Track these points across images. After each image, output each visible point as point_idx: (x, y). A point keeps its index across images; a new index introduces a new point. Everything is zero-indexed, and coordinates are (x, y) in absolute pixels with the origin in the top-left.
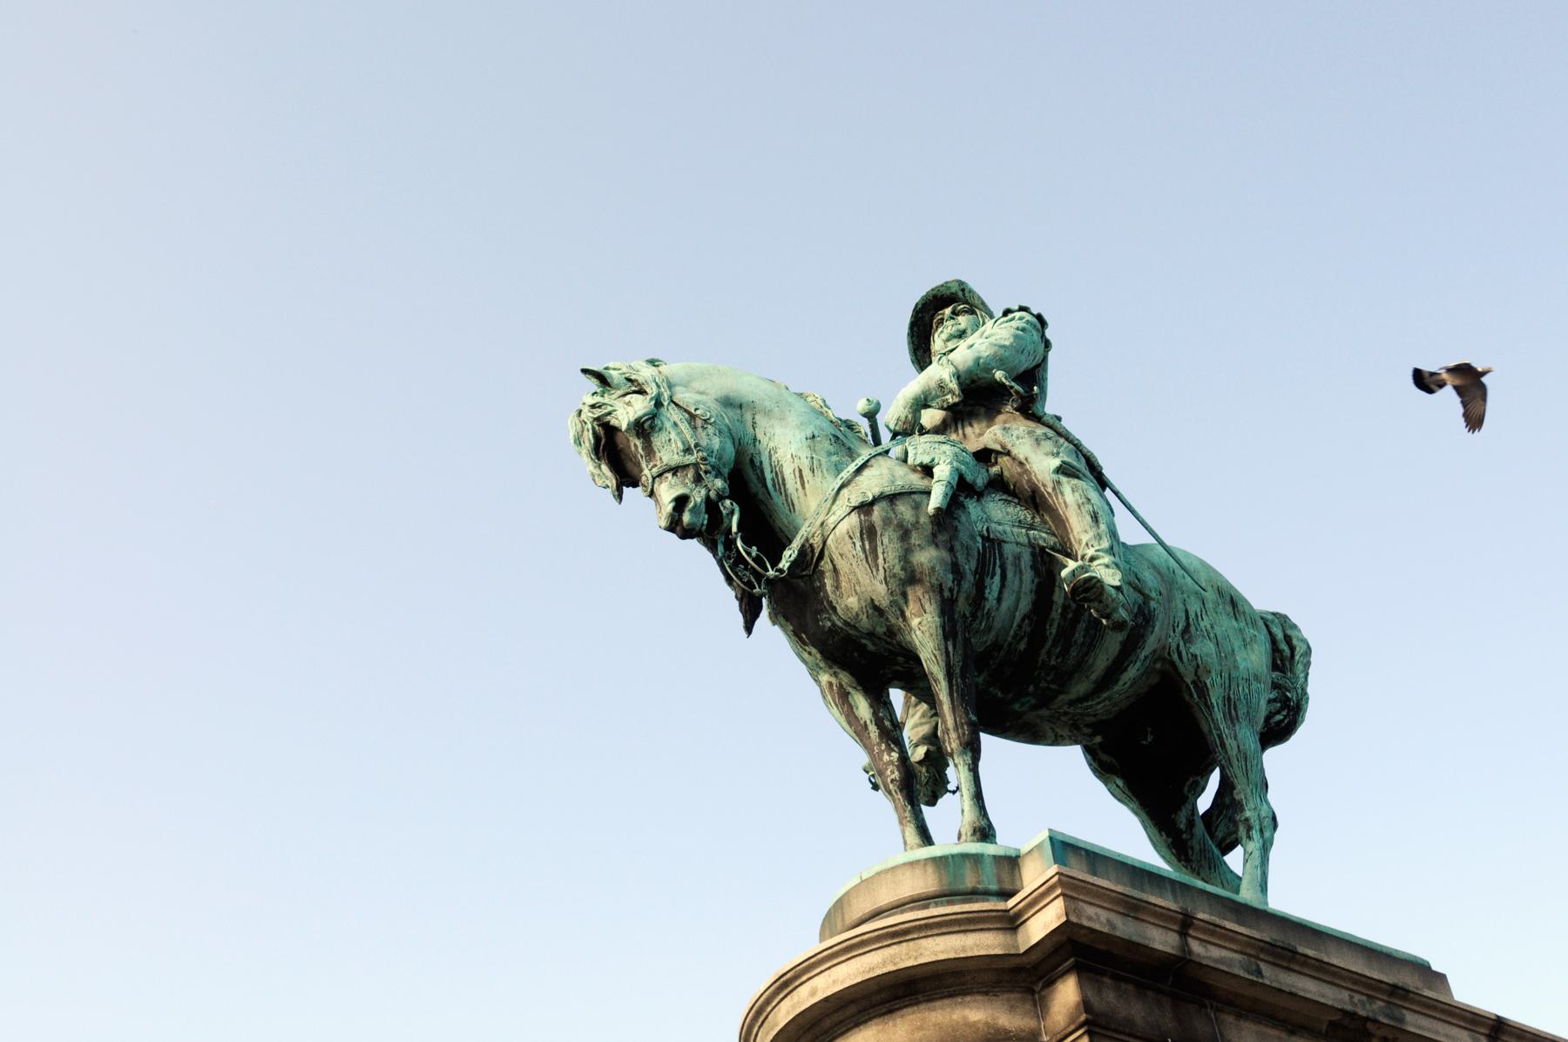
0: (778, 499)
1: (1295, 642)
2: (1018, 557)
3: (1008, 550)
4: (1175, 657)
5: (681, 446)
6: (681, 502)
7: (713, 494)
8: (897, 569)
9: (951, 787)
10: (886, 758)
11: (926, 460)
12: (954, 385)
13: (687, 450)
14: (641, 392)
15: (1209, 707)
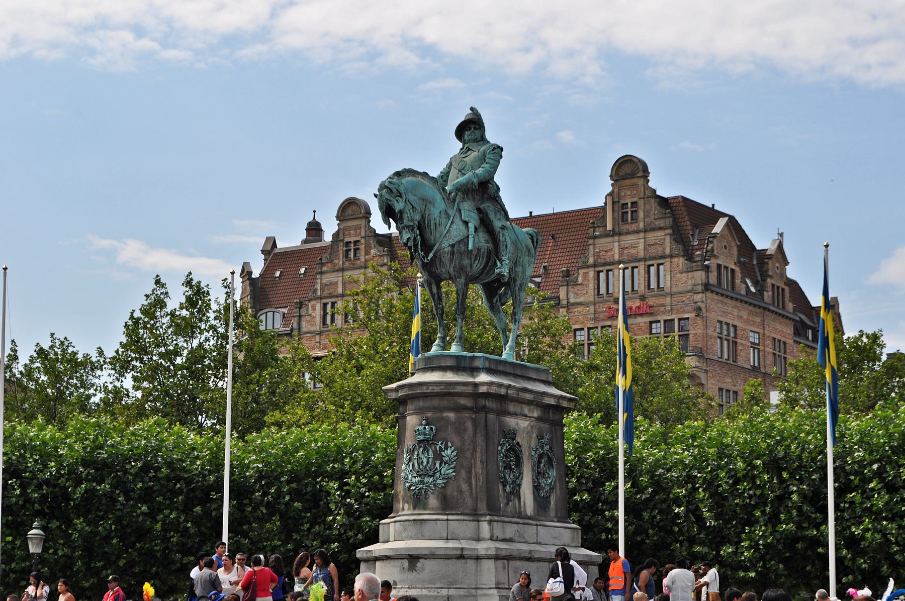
2: (484, 254)
3: (482, 250)
12: (477, 185)
14: (401, 196)
15: (515, 285)
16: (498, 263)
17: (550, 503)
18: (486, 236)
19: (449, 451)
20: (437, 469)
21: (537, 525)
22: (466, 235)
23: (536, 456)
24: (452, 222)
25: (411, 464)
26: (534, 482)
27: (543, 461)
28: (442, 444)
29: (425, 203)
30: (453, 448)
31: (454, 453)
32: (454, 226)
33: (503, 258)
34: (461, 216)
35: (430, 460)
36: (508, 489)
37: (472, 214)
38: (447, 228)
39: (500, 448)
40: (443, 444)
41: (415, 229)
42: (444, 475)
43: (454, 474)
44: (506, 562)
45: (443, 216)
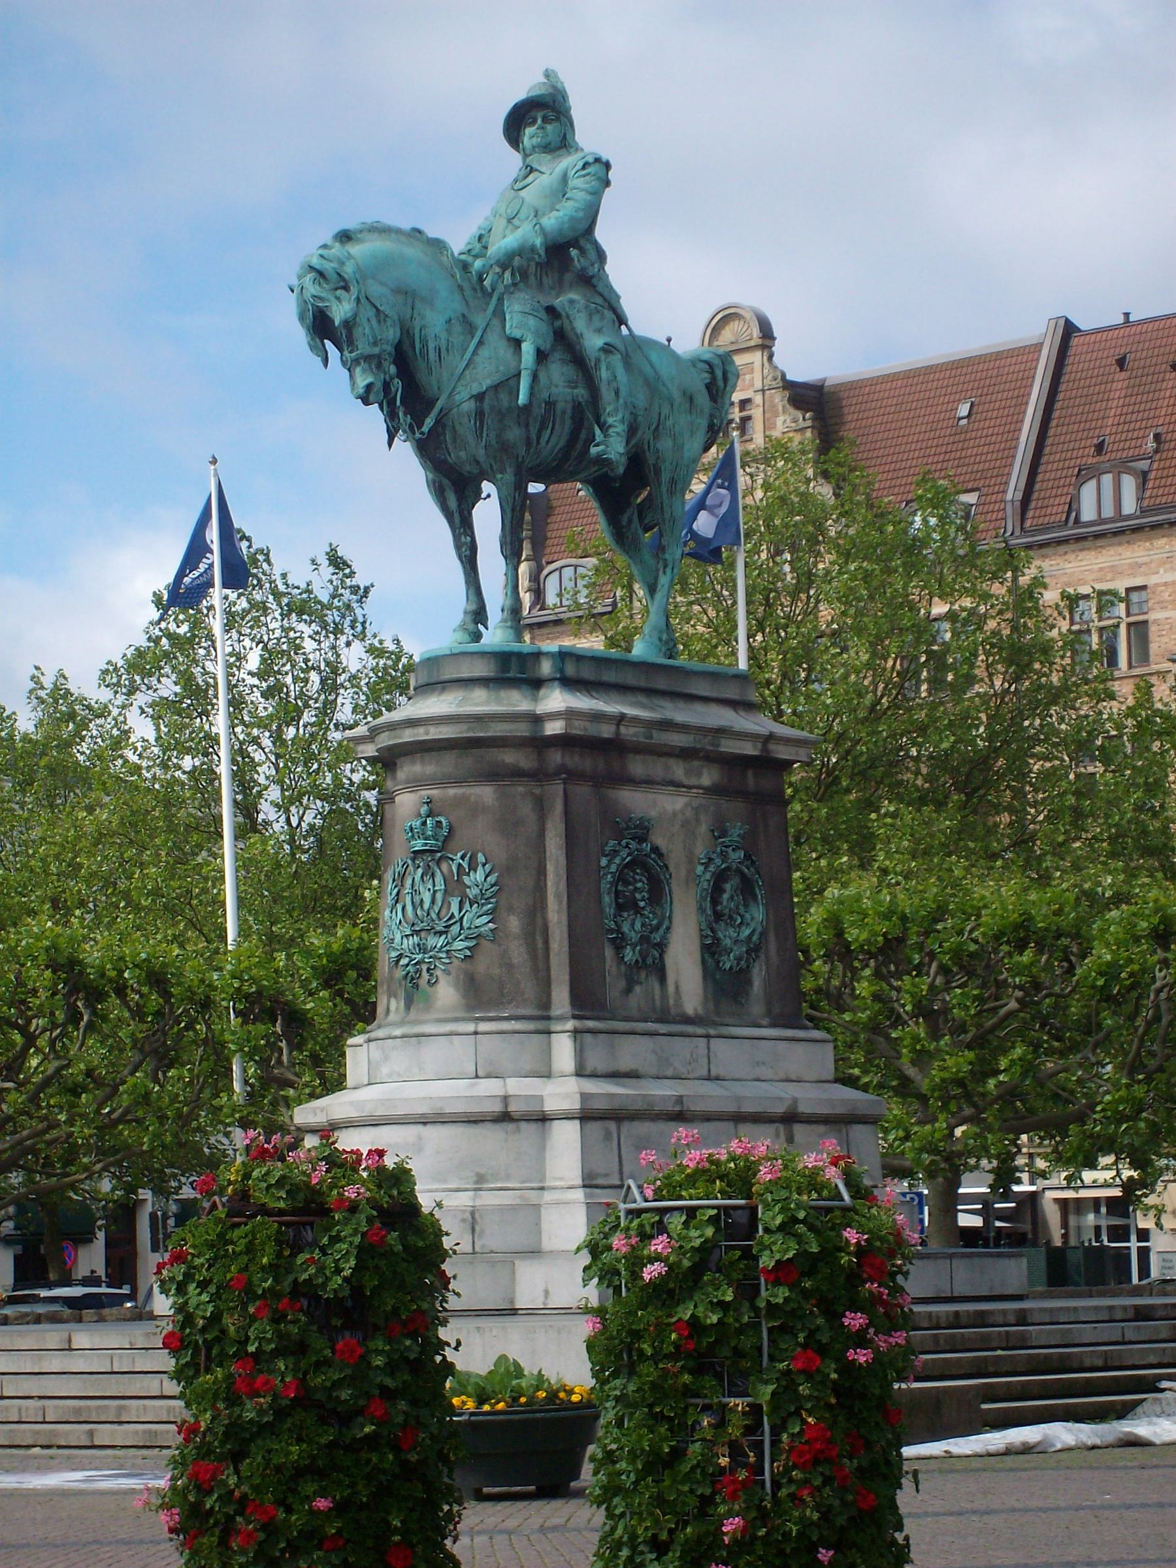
0: (421, 364)
1: (729, 375)
3: (560, 406)
4: (646, 447)
5: (371, 340)
6: (369, 387)
7: (388, 379)
8: (494, 443)
9: (483, 495)
10: (463, 538)
11: (518, 336)
12: (542, 252)
13: (375, 344)
14: (346, 288)
16: (598, 431)
17: (749, 982)
18: (570, 371)
19: (479, 875)
20: (452, 916)
21: (708, 1036)
22: (513, 371)
23: (708, 876)
24: (481, 343)
25: (399, 907)
26: (703, 937)
27: (728, 886)
28: (463, 858)
29: (410, 300)
31: (492, 879)
32: (484, 352)
33: (610, 420)
34: (504, 327)
35: (439, 896)
36: (629, 955)
37: (532, 321)
38: (468, 356)
39: (604, 862)
40: (467, 859)
41: (385, 364)
42: (469, 928)
44: (612, 1126)
45: (457, 328)
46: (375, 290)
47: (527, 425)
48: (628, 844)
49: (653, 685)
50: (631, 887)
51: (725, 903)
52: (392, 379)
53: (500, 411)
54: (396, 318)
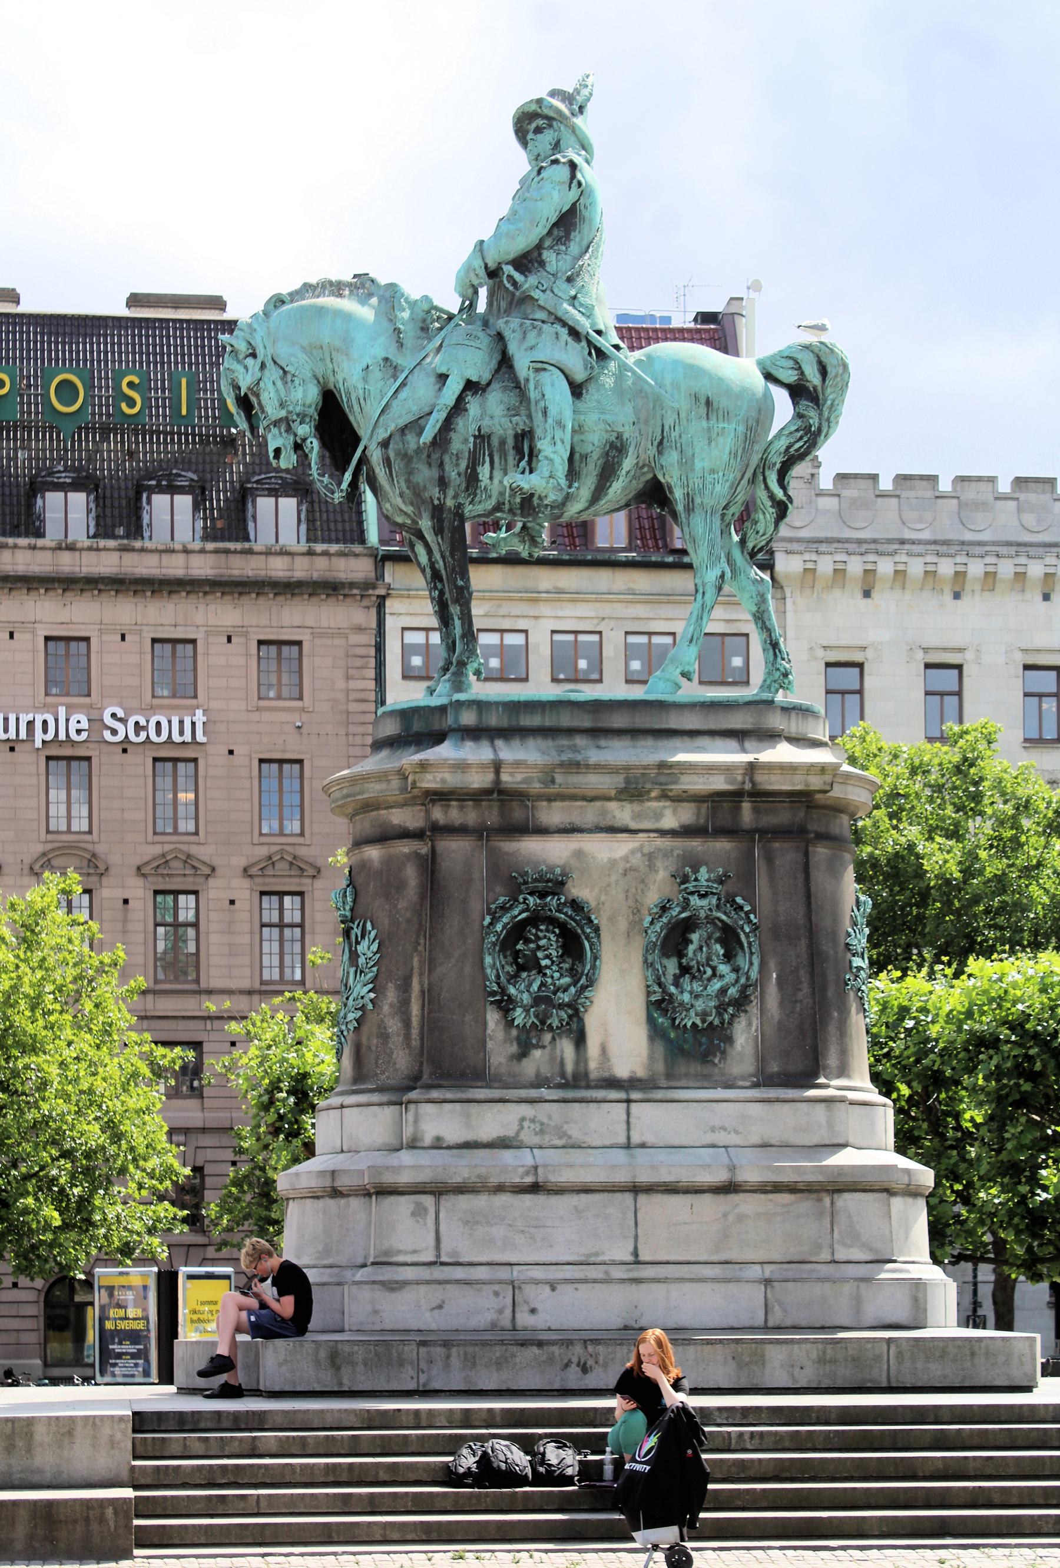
11: (443, 370)
14: (254, 355)
19: (365, 943)
24: (403, 384)
30: (373, 934)
31: (375, 947)
36: (519, 1016)
38: (384, 403)
43: (372, 995)
44: (428, 1201)
46: (285, 352)
47: (441, 465)
48: (525, 899)
49: (601, 725)
50: (532, 946)
51: (690, 954)
52: (304, 440)
53: (406, 455)
54: (309, 375)
